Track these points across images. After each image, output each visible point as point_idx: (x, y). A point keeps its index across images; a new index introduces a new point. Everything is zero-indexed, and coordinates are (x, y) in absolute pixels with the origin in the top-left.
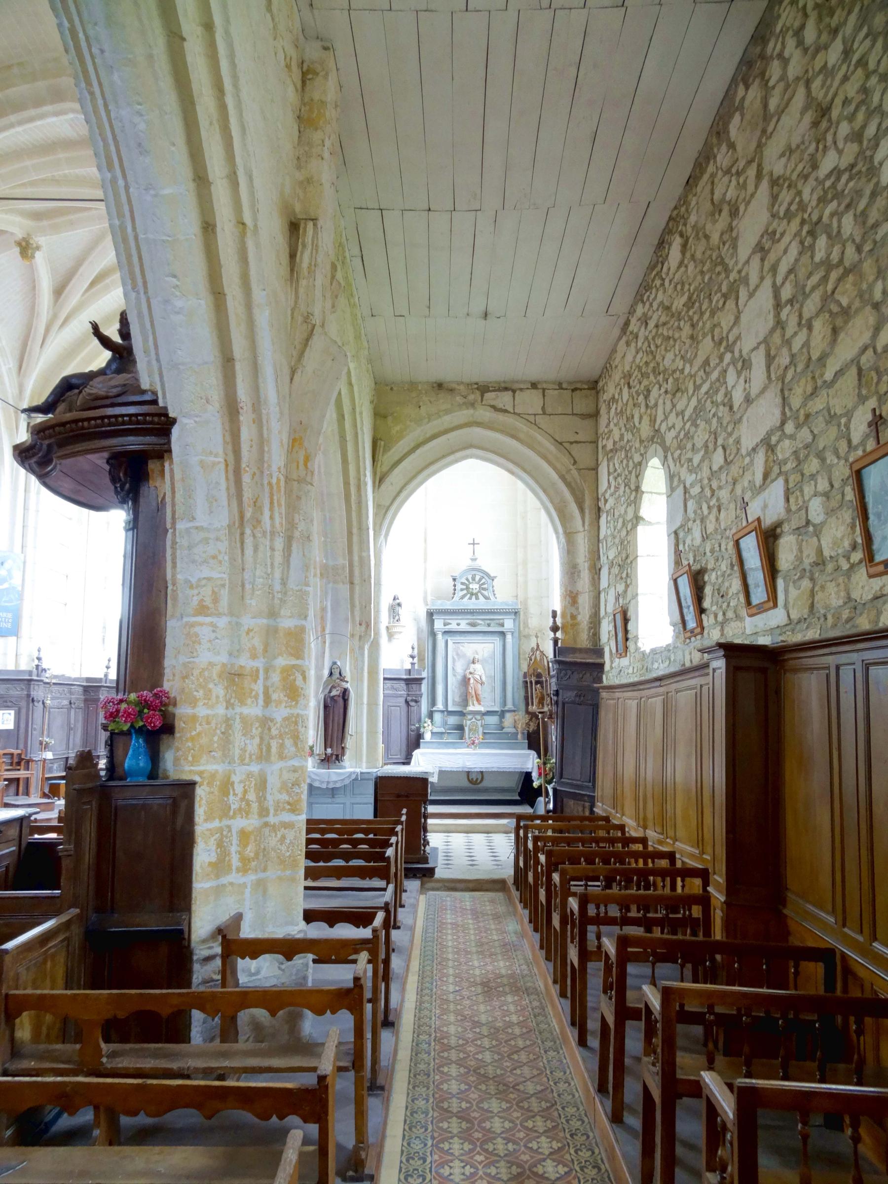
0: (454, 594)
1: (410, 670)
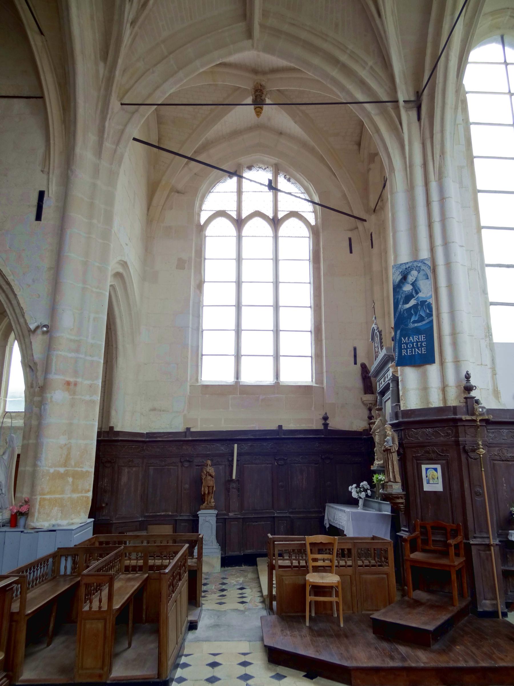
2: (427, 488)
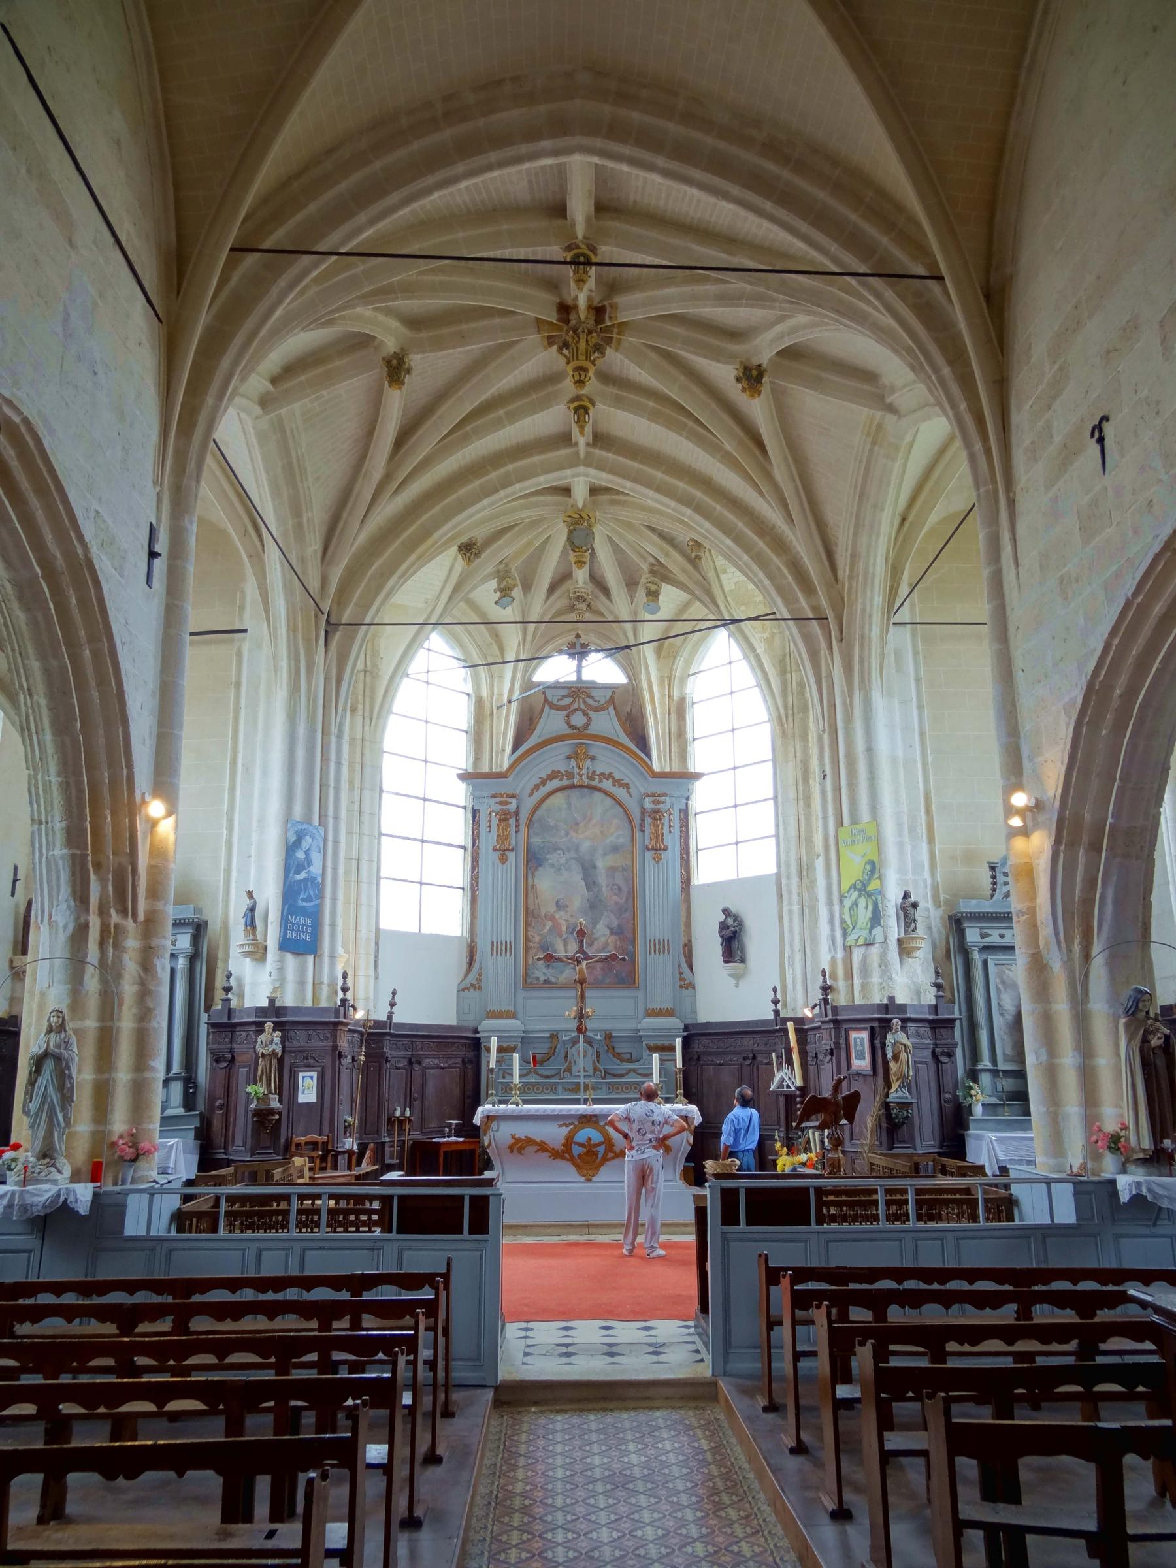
0: (994, 890)
1: (936, 1007)
2: (301, 1099)
